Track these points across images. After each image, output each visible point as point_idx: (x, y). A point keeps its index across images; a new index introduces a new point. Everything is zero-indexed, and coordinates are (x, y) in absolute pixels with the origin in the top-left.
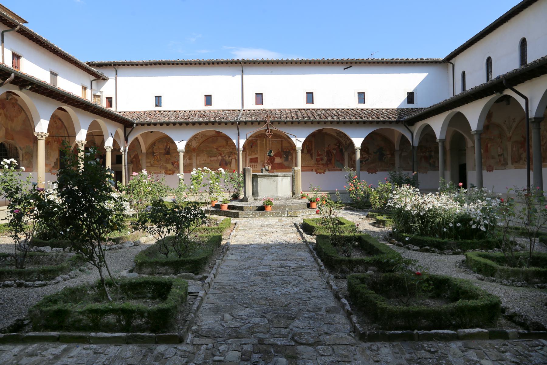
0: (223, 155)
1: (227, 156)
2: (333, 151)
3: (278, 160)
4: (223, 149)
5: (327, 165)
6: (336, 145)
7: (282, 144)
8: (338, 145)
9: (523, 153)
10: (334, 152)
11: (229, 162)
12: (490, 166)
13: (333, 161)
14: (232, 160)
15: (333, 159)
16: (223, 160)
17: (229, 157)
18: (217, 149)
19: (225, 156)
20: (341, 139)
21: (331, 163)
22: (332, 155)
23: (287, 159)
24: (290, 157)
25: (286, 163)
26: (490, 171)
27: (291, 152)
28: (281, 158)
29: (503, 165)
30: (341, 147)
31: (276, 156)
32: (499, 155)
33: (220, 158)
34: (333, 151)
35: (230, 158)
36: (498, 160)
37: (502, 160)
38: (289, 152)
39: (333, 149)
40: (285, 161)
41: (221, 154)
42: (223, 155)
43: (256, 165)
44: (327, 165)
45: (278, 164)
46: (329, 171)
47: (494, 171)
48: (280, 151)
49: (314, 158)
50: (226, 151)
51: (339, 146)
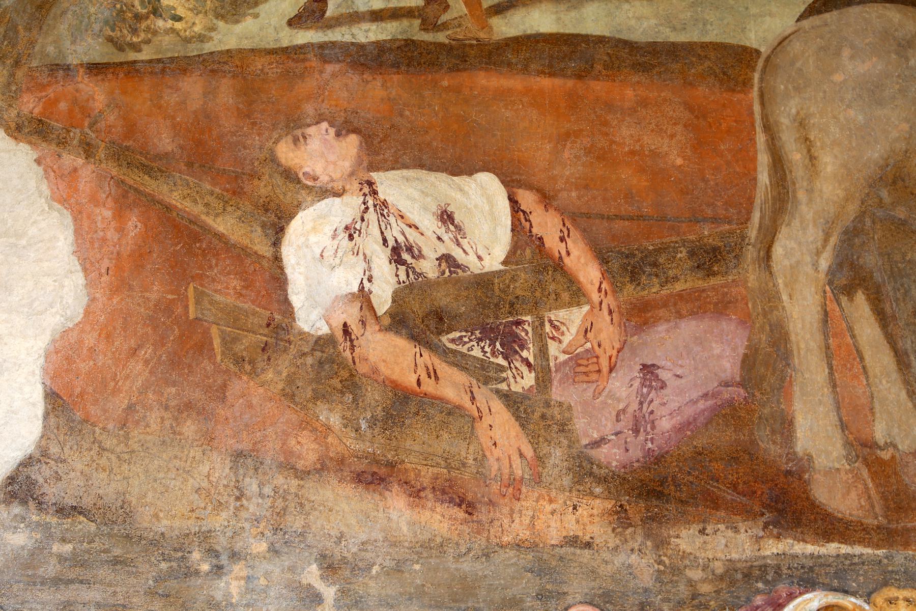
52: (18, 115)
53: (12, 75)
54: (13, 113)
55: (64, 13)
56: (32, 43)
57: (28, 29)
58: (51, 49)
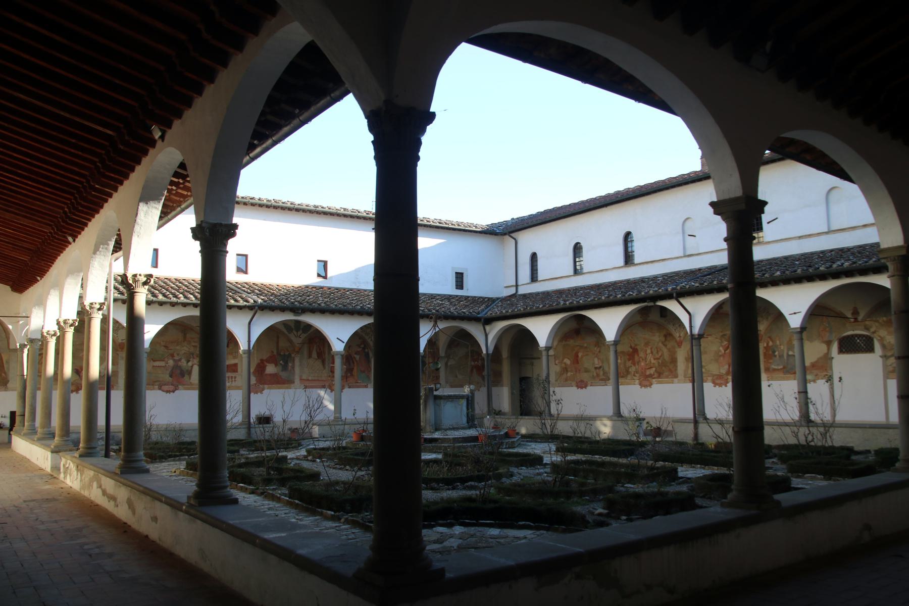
0: (177, 358)
1: (184, 361)
2: (355, 356)
3: (270, 369)
4: (178, 348)
5: (346, 379)
6: (359, 346)
7: (278, 343)
8: (362, 346)
9: (631, 366)
10: (357, 357)
11: (187, 370)
12: (582, 381)
13: (355, 372)
14: (192, 366)
15: (355, 368)
16: (176, 367)
17: (188, 361)
18: (166, 347)
19: (180, 360)
20: (367, 338)
21: (352, 375)
22: (354, 363)
23: (285, 368)
24: (290, 364)
25: (284, 375)
26: (582, 388)
27: (293, 355)
28: (276, 365)
29: (602, 380)
30: (366, 350)
31: (269, 363)
32: (596, 368)
33: (171, 362)
34: (355, 356)
35: (190, 364)
36: (595, 374)
37: (601, 373)
38: (290, 355)
39: (356, 354)
40: (282, 371)
41: (172, 355)
42: (177, 358)
43: (235, 377)
44: (346, 379)
45: (270, 375)
46: (349, 387)
47: (589, 388)
48: (275, 353)
49: (327, 367)
50: (183, 352)
51: (364, 348)
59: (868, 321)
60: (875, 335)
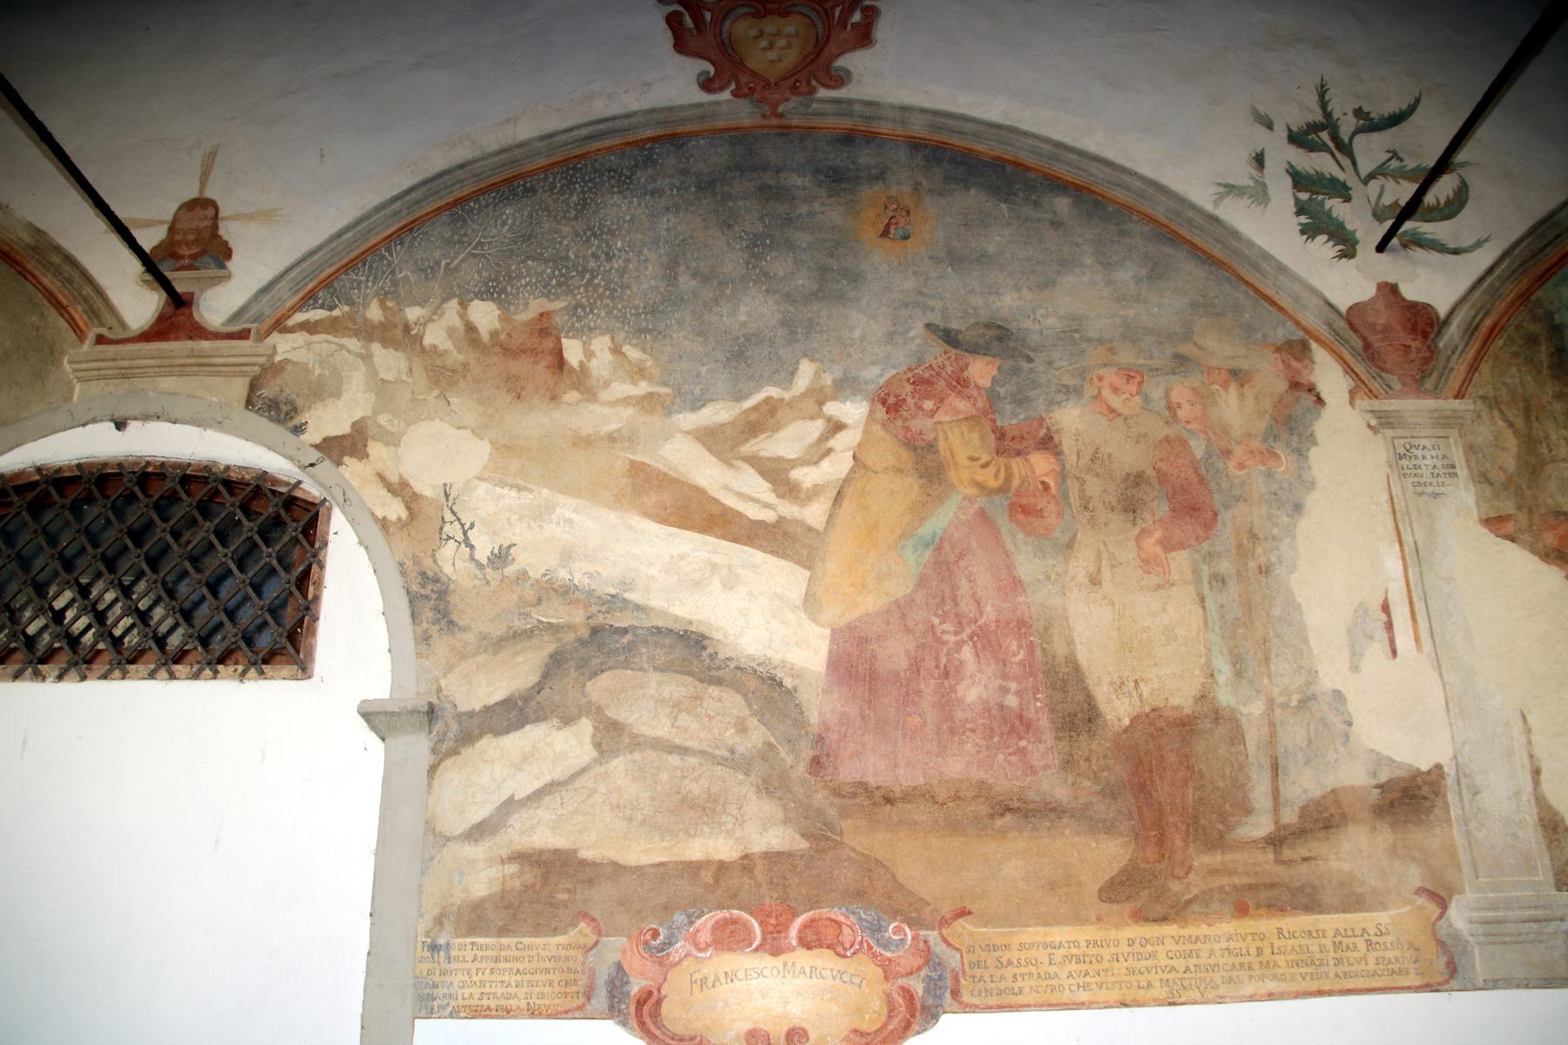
52: (1545, 546)
53: (1531, 519)
54: (1541, 545)
55: (1549, 477)
56: (1535, 498)
57: (1530, 488)
58: (1550, 501)
59: (306, 327)
60: (352, 469)
